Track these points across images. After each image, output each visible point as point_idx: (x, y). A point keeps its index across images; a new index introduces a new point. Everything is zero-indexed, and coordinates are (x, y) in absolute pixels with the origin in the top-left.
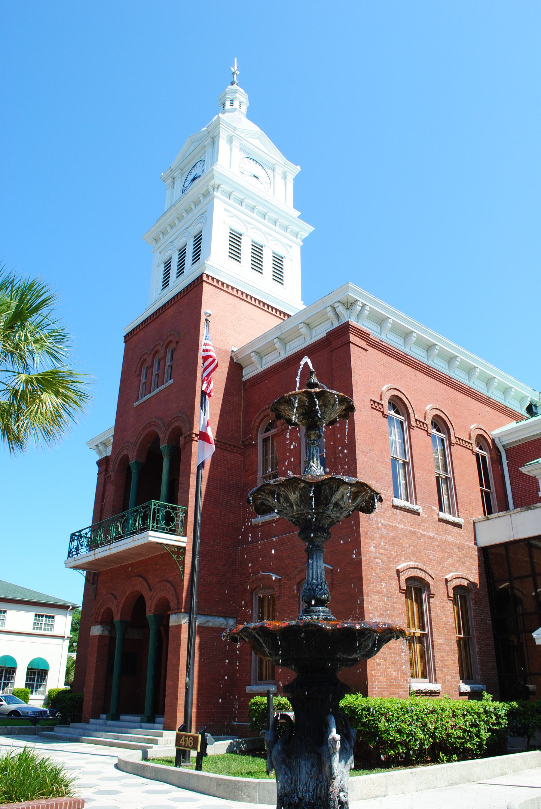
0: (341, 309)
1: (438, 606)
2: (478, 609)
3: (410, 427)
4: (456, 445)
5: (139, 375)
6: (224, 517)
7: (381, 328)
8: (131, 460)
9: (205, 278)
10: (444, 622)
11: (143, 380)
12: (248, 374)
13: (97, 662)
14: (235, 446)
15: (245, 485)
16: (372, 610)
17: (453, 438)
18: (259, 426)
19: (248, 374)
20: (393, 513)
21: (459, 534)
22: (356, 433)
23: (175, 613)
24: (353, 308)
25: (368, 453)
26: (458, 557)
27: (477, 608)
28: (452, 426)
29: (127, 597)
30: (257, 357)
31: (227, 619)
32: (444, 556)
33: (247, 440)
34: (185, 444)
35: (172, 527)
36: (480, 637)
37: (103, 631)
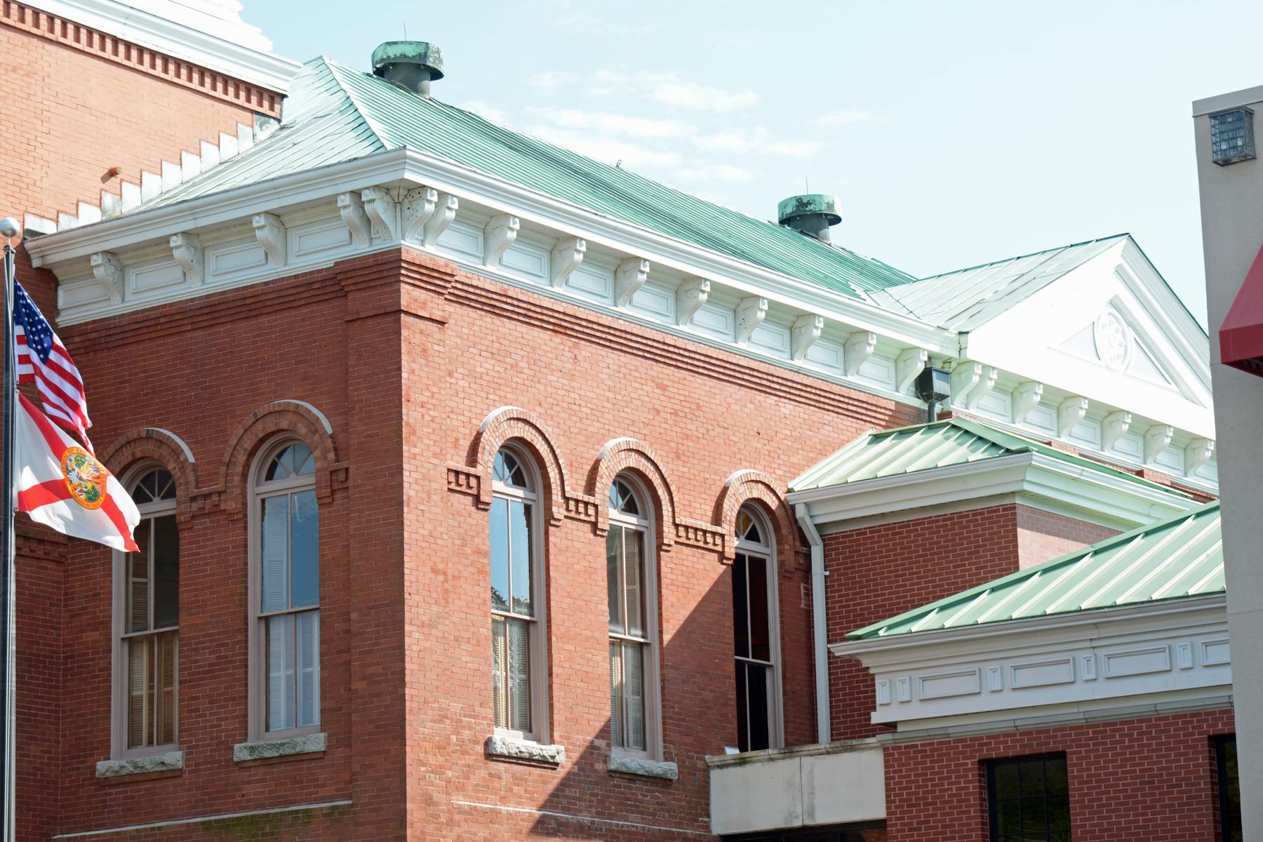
0: (379, 207)
3: (549, 518)
4: (676, 548)
15: (72, 657)
17: (668, 530)
20: (490, 775)
21: (662, 804)
22: (406, 577)
24: (414, 204)
28: (670, 494)
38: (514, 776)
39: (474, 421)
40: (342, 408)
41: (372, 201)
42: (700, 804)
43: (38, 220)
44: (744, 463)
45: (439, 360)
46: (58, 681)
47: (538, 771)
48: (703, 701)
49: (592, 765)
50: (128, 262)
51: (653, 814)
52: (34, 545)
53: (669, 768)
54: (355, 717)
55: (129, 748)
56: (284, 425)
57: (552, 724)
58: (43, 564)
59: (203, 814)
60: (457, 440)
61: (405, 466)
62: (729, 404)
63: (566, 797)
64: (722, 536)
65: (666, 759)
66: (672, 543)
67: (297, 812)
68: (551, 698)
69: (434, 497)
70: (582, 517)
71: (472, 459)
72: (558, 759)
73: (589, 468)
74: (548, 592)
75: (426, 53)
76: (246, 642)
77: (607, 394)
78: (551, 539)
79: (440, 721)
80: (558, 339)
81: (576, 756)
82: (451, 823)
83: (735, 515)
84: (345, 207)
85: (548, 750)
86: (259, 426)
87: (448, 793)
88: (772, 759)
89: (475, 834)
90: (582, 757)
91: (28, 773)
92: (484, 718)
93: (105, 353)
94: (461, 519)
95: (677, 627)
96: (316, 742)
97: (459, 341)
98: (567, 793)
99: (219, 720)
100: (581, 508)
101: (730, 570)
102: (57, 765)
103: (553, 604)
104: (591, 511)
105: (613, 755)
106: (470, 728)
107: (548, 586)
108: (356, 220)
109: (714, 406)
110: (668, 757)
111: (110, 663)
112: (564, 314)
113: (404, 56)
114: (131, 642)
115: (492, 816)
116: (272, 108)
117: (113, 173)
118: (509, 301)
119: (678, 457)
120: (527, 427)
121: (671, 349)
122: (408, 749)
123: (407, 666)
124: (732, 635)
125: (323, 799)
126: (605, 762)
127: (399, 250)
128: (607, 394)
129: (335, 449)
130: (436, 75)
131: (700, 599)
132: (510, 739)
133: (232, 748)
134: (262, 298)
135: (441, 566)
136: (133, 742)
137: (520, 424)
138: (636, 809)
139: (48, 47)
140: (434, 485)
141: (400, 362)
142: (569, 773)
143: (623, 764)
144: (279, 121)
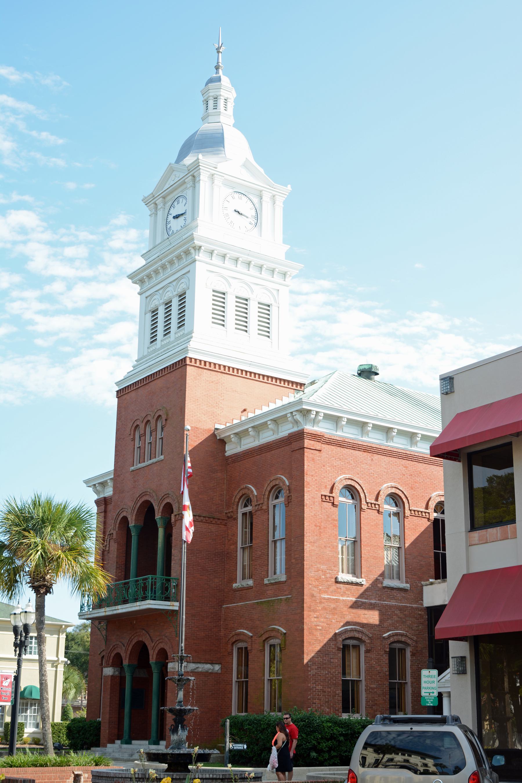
1: (373, 659)
2: (415, 660)
5: (134, 440)
6: (210, 582)
7: (337, 425)
8: (130, 523)
9: (188, 362)
10: (378, 671)
11: (137, 445)
12: (231, 450)
13: (110, 698)
14: (219, 519)
15: (228, 553)
16: (311, 665)
18: (238, 502)
19: (231, 450)
20: (337, 588)
22: (305, 528)
23: (171, 662)
25: (316, 543)
26: (399, 618)
27: (414, 658)
28: (408, 500)
29: (134, 645)
30: (236, 439)
31: (214, 665)
32: (383, 618)
33: (229, 512)
34: (176, 521)
35: (167, 595)
36: (415, 682)
37: (114, 672)
38: (346, 588)
39: (333, 480)
40: (290, 477)
41: (296, 415)
42: (419, 597)
43: (219, 425)
44: (438, 490)
45: (319, 462)
46: (225, 560)
47: (356, 587)
48: (421, 565)
49: (377, 585)
50: (242, 436)
51: (401, 600)
52: (217, 520)
53: (407, 586)
54: (292, 571)
55: (243, 580)
56: (277, 483)
57: (361, 572)
58: (220, 526)
59: (256, 600)
60: (326, 486)
61: (305, 494)
62: (433, 472)
63: (366, 595)
64: (429, 513)
65: (406, 583)
66: (409, 515)
67: (278, 599)
68: (361, 564)
69: (316, 503)
70: (374, 508)
71: (331, 491)
72: (362, 583)
73: (377, 493)
74: (361, 532)
75: (371, 367)
76: (268, 548)
77: (384, 470)
78: (362, 515)
79: (317, 572)
80: (366, 454)
81: (371, 582)
82: (321, 603)
83: (434, 506)
84: (289, 417)
85: (359, 580)
86: (271, 483)
87: (320, 593)
88: (439, 583)
89: (330, 606)
90: (373, 582)
91: (215, 587)
92: (335, 571)
93: (237, 463)
94: (327, 510)
95: (411, 542)
96: (283, 578)
97: (328, 456)
98: (367, 593)
99: (262, 571)
100: (373, 505)
101: (432, 523)
102: (224, 585)
103: (362, 535)
104: (377, 506)
105: (384, 582)
106: (330, 574)
107: (361, 530)
108: (293, 421)
109: (426, 473)
110: (407, 582)
111: (237, 555)
112: (367, 446)
113: (365, 369)
114: (243, 549)
115: (337, 601)
116: (301, 388)
117: (245, 410)
118: (346, 443)
119: (412, 489)
120: (352, 481)
121: (409, 455)
122: (305, 580)
123: (305, 555)
124: (433, 544)
125: (285, 595)
126: (382, 584)
127: (303, 429)
128: (384, 470)
129: (289, 490)
130: (377, 374)
131: (420, 533)
132: (345, 577)
133: (264, 580)
134: (272, 445)
135: (318, 524)
136: (244, 578)
137: (350, 480)
138: (394, 598)
139: (223, 375)
140: (316, 500)
141: (304, 463)
142: (368, 587)
143: (388, 585)
144: (303, 391)
